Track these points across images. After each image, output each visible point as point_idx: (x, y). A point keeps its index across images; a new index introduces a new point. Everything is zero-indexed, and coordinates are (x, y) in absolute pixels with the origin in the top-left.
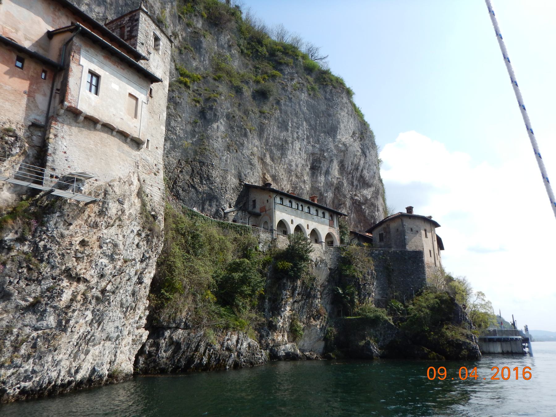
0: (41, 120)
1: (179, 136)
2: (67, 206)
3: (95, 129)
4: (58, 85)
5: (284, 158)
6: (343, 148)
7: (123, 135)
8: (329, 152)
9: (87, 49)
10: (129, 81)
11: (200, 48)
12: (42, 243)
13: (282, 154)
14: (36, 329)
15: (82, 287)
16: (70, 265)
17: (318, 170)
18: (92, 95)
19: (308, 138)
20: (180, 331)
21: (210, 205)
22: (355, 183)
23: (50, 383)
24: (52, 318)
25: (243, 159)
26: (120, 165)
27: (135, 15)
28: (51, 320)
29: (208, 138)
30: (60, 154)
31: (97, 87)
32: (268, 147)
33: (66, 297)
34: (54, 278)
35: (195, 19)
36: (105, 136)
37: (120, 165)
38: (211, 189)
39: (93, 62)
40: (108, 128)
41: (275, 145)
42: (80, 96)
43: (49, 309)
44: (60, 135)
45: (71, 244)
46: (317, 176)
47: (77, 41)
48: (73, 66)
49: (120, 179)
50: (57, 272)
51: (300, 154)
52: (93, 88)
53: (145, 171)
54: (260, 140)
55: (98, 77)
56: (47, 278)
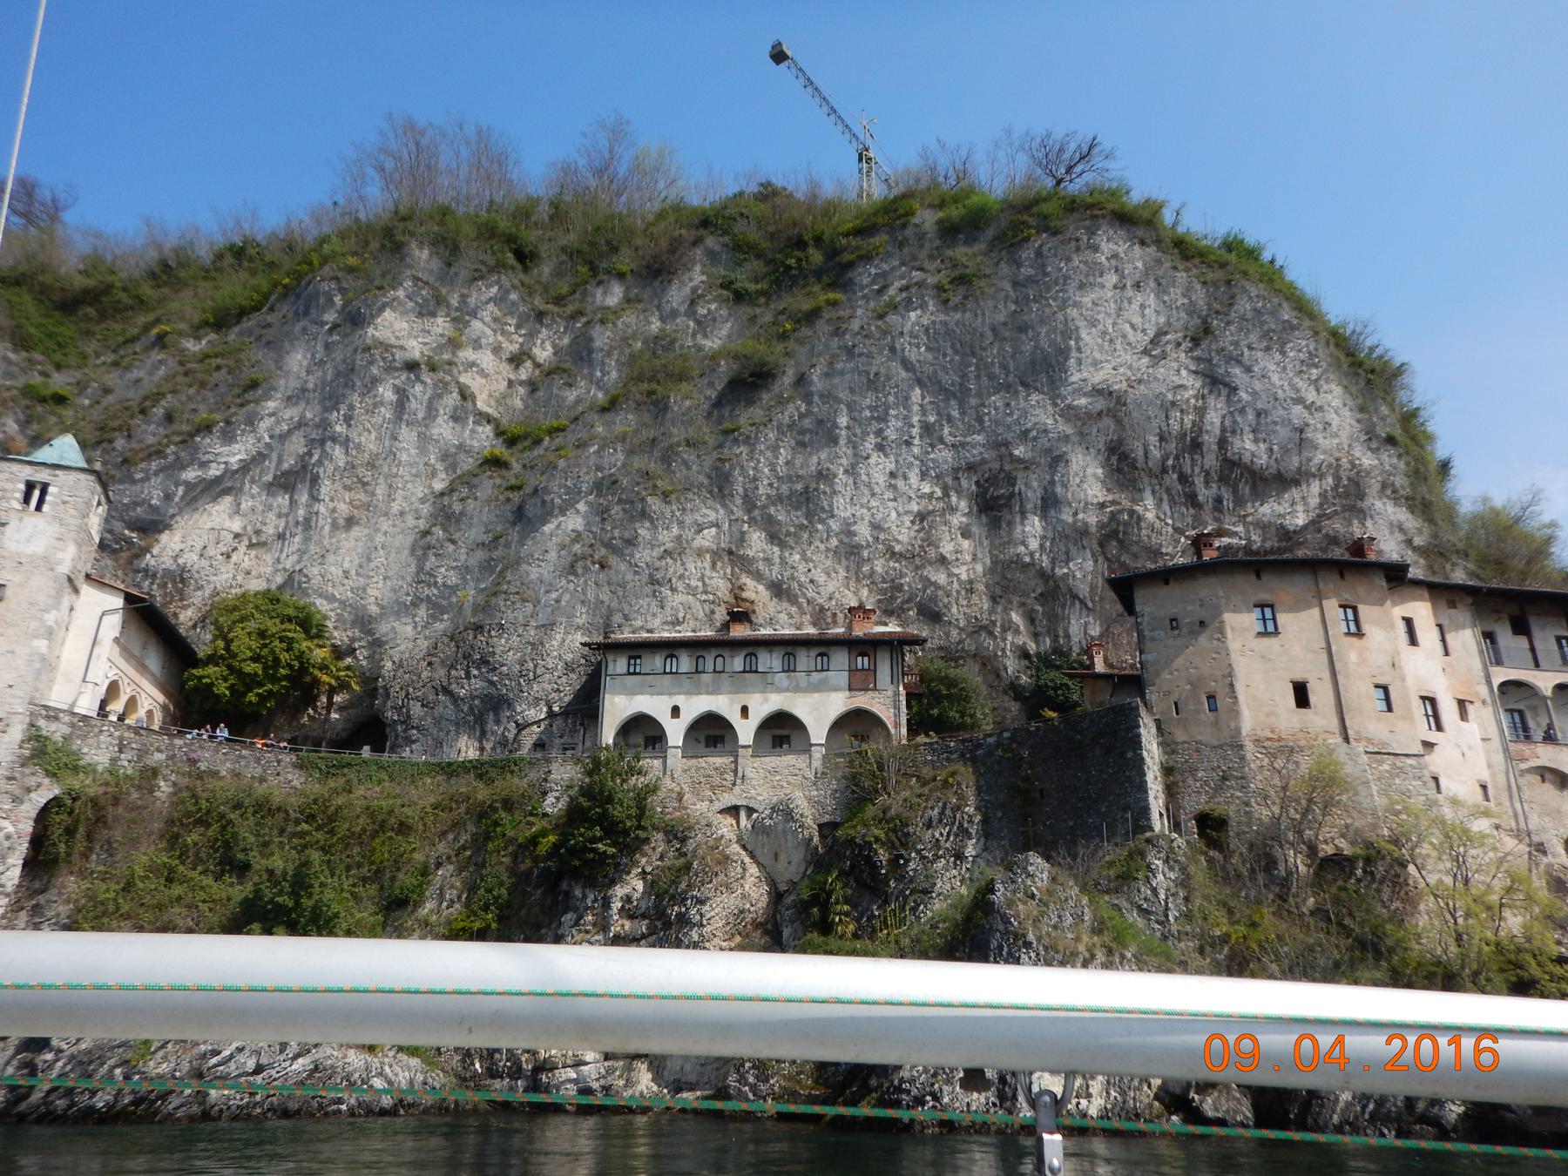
1: (444, 585)
5: (822, 521)
6: (1100, 404)
8: (1035, 439)
11: (590, 351)
13: (809, 515)
17: (1009, 506)
19: (927, 429)
22: (1204, 494)
25: (629, 577)
32: (756, 512)
35: (599, 293)
38: (492, 683)
41: (779, 499)
46: (1010, 524)
51: (894, 487)
54: (724, 506)
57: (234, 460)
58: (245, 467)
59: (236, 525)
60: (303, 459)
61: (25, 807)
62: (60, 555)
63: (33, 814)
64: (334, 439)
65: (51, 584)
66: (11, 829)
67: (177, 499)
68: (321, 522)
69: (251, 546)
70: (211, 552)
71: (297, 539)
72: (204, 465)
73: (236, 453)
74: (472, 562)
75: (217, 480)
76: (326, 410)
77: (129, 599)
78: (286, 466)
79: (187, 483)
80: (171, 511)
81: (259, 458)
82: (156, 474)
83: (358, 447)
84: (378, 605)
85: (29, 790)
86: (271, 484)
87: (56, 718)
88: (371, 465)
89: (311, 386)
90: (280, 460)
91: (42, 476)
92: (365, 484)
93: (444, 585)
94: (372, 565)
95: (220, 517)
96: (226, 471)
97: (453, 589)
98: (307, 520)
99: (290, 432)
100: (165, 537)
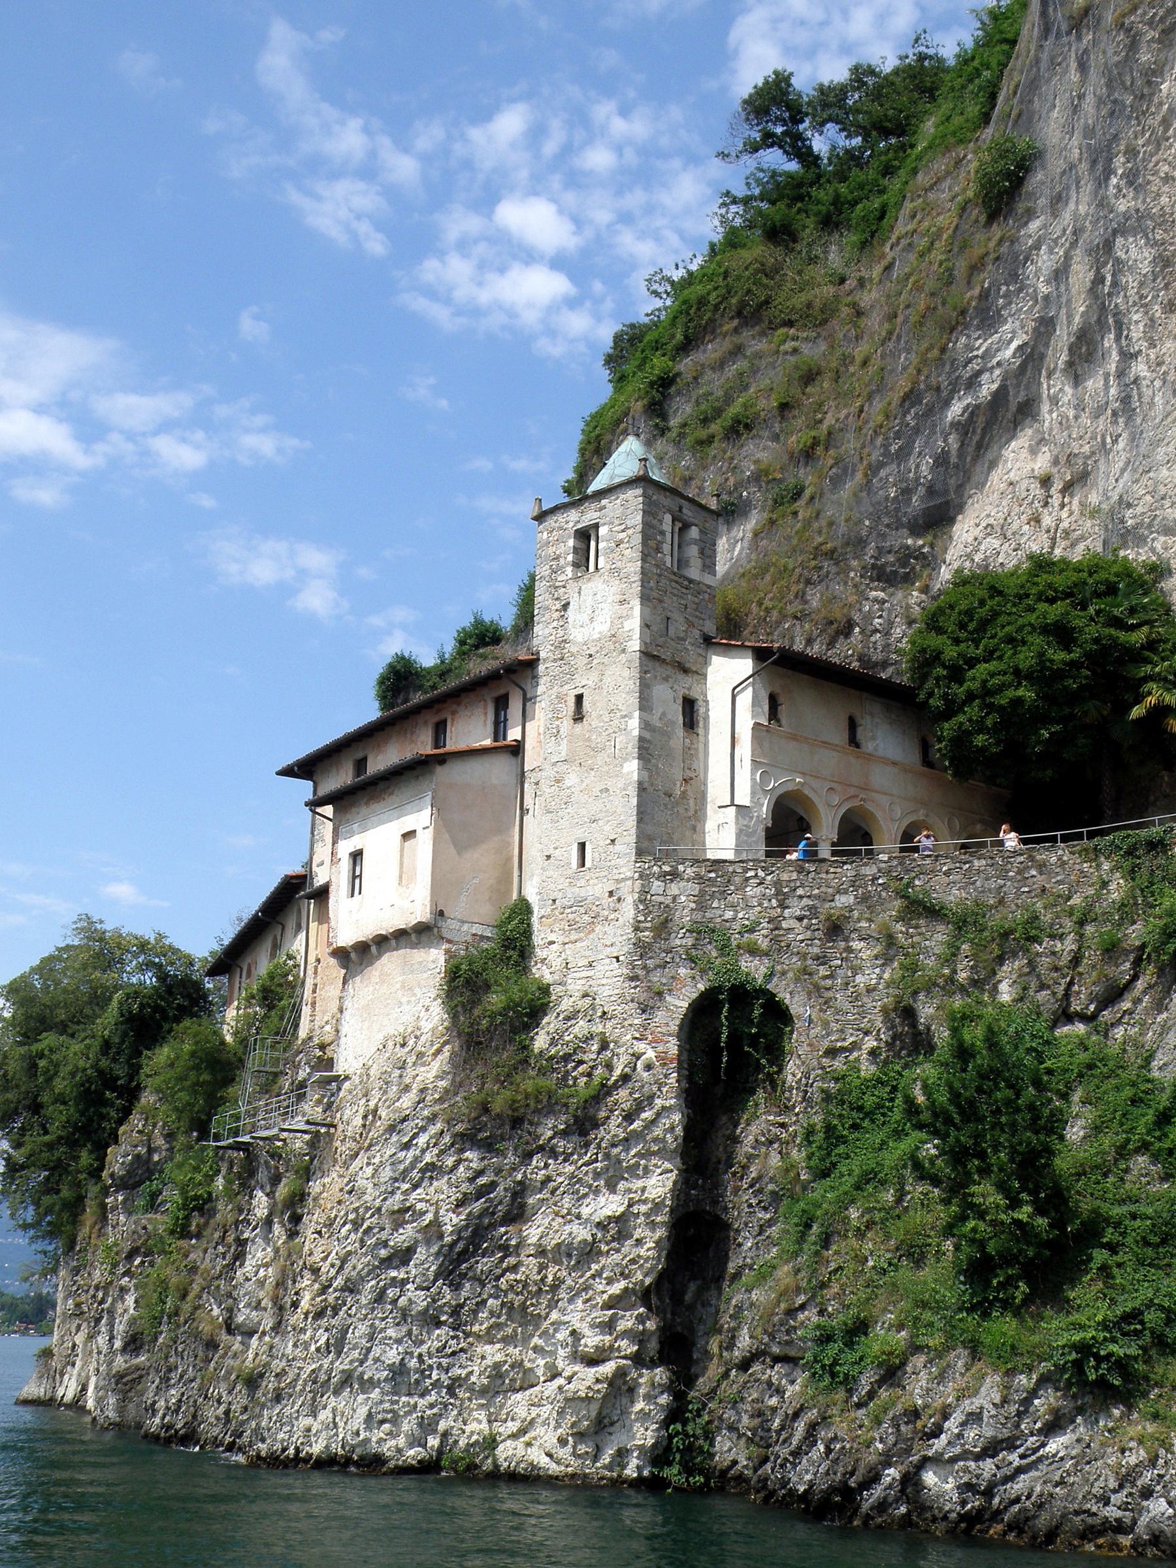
10: (401, 810)
40: (383, 942)
58: (1032, 357)
59: (1042, 463)
61: (660, 1016)
62: (628, 625)
63: (674, 1027)
64: (1121, 231)
65: (626, 673)
66: (651, 1054)
67: (954, 459)
68: (1147, 392)
69: (1068, 488)
71: (1121, 444)
72: (972, 383)
73: (1008, 342)
75: (1000, 397)
77: (761, 655)
79: (955, 425)
80: (952, 482)
81: (1045, 326)
82: (917, 431)
85: (660, 994)
87: (675, 875)
95: (1019, 461)
96: (1004, 379)
98: (1126, 400)
99: (1068, 257)
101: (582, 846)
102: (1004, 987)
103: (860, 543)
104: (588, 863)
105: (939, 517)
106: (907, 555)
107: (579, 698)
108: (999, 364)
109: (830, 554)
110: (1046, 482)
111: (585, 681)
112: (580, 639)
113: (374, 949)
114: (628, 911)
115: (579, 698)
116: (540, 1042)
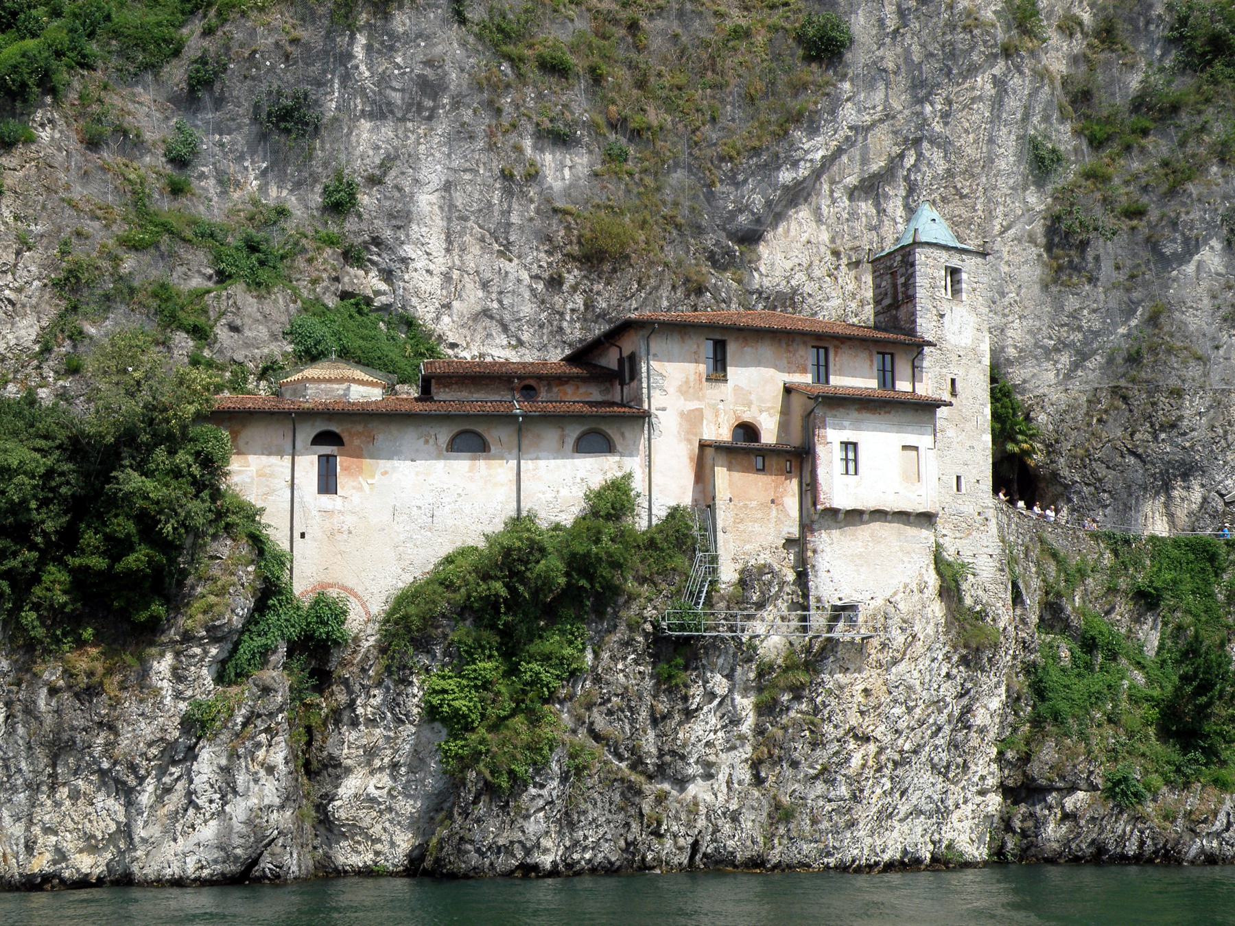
0: (795, 532)
1: (1089, 330)
2: (840, 647)
3: (862, 523)
4: (807, 479)
7: (903, 517)
9: (834, 412)
10: (900, 427)
12: (819, 700)
14: (830, 801)
15: (872, 748)
16: (853, 722)
18: (851, 479)
20: (1080, 795)
21: (1188, 488)
23: (854, 861)
24: (843, 788)
26: (903, 562)
27: (909, 254)
28: (843, 790)
29: (1169, 308)
30: (822, 574)
31: (856, 460)
33: (856, 761)
34: (839, 741)
36: (876, 526)
37: (903, 562)
39: (845, 428)
40: (879, 515)
42: (837, 489)
43: (839, 778)
44: (820, 548)
45: (852, 696)
47: (819, 412)
48: (820, 450)
49: (906, 586)
50: (841, 732)
52: (851, 465)
53: (958, 535)
55: (855, 445)
56: (832, 741)
57: (818, 155)
60: (895, 162)
70: (817, 273)
72: (795, 164)
74: (1113, 304)
76: (921, 102)
78: (874, 168)
83: (959, 152)
84: (1016, 347)
86: (856, 187)
88: (969, 173)
89: (891, 66)
90: (865, 161)
91: (955, 262)
92: (962, 197)
93: (1089, 330)
94: (1006, 301)
97: (1097, 334)
100: (762, 249)
101: (958, 478)
102: (1077, 598)
103: (699, 230)
104: (963, 490)
105: (751, 238)
106: (729, 253)
107: (953, 381)
108: (811, 161)
109: (678, 227)
110: (836, 254)
111: (958, 371)
112: (953, 342)
113: (866, 517)
114: (993, 527)
115: (953, 381)
116: (968, 601)
